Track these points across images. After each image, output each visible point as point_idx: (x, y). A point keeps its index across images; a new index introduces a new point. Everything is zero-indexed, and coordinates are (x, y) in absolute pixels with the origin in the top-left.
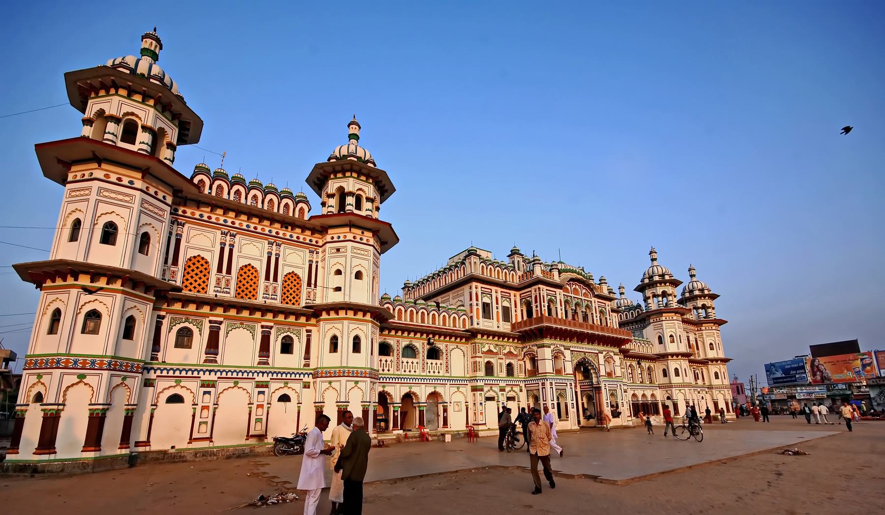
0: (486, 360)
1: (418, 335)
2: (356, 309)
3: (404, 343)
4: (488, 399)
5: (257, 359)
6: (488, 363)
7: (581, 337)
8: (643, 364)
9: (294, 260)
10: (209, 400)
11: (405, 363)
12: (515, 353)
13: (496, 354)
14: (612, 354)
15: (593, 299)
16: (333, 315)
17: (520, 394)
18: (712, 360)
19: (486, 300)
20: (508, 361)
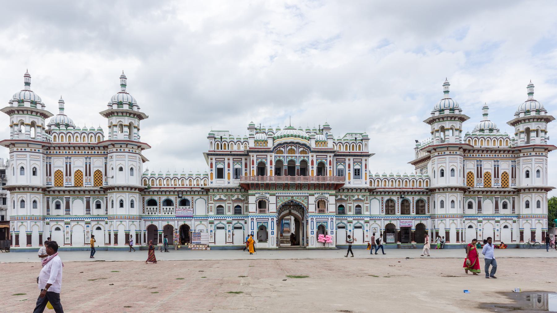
0: (218, 205)
1: (172, 193)
2: (118, 188)
3: (164, 198)
4: (218, 228)
5: (85, 212)
6: (220, 206)
7: (286, 187)
8: (410, 198)
9: (97, 163)
10: (69, 230)
11: (165, 209)
12: (243, 199)
13: (225, 201)
14: (327, 196)
15: (310, 155)
16: (111, 191)
17: (245, 225)
18: (524, 189)
19: (220, 166)
20: (236, 205)
